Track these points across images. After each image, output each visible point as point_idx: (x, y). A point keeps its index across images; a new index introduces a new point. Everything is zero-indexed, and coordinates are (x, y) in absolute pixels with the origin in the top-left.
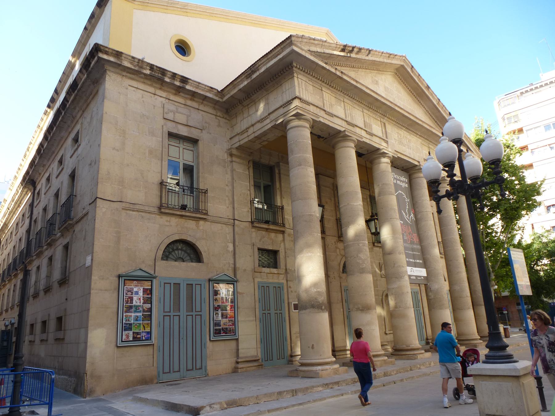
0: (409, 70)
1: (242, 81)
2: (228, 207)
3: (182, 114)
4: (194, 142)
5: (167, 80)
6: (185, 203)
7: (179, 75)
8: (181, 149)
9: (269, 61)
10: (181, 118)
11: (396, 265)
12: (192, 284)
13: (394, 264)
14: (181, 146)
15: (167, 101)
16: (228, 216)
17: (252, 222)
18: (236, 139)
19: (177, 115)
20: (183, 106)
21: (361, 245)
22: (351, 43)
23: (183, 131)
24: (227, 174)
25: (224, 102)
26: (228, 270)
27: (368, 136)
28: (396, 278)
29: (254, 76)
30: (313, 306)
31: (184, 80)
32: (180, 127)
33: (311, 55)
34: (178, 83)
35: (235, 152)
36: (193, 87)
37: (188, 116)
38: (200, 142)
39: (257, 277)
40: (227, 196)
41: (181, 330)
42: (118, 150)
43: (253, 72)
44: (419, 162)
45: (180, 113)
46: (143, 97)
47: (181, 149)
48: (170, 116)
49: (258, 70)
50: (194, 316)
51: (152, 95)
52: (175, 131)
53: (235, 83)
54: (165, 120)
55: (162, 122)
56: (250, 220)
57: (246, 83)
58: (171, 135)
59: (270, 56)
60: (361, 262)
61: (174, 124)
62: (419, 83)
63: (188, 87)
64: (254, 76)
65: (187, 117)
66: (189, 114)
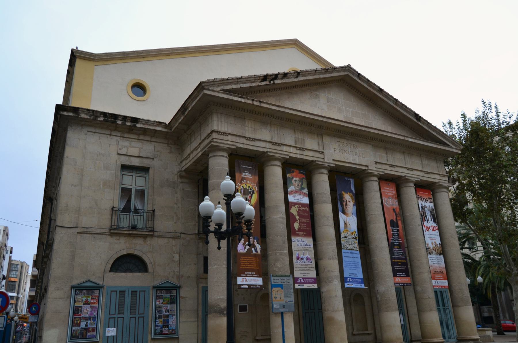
0: (356, 78)
1: (180, 116)
2: (175, 223)
3: (135, 147)
4: (145, 170)
5: (119, 122)
6: (136, 224)
7: (129, 117)
8: (134, 177)
9: (193, 102)
10: (134, 151)
11: (325, 271)
12: (137, 291)
13: (324, 269)
14: (134, 174)
15: (122, 138)
16: (175, 231)
17: (199, 234)
18: (184, 163)
19: (130, 149)
20: (136, 140)
21: (278, 254)
22: (270, 72)
23: (136, 162)
24: (176, 193)
25: (173, 132)
26: (173, 277)
27: (298, 152)
28: (326, 282)
29: (186, 113)
30: (216, 312)
31: (135, 120)
32: (132, 158)
33: (224, 94)
34: (128, 124)
35: (184, 173)
36: (143, 124)
37: (140, 149)
38: (150, 169)
39: (202, 283)
40: (175, 213)
41: (125, 330)
42: (76, 186)
43: (186, 110)
44: (367, 166)
45: (133, 147)
46: (100, 139)
47: (134, 177)
48: (124, 151)
49: (188, 108)
50: (116, 319)
51: (109, 136)
52: (127, 163)
53: (176, 117)
54: (119, 156)
55: (117, 157)
56: (197, 232)
57: (182, 118)
58: (124, 167)
59: (192, 97)
60: (276, 269)
61: (127, 158)
62: (369, 88)
63: (138, 125)
64: (186, 113)
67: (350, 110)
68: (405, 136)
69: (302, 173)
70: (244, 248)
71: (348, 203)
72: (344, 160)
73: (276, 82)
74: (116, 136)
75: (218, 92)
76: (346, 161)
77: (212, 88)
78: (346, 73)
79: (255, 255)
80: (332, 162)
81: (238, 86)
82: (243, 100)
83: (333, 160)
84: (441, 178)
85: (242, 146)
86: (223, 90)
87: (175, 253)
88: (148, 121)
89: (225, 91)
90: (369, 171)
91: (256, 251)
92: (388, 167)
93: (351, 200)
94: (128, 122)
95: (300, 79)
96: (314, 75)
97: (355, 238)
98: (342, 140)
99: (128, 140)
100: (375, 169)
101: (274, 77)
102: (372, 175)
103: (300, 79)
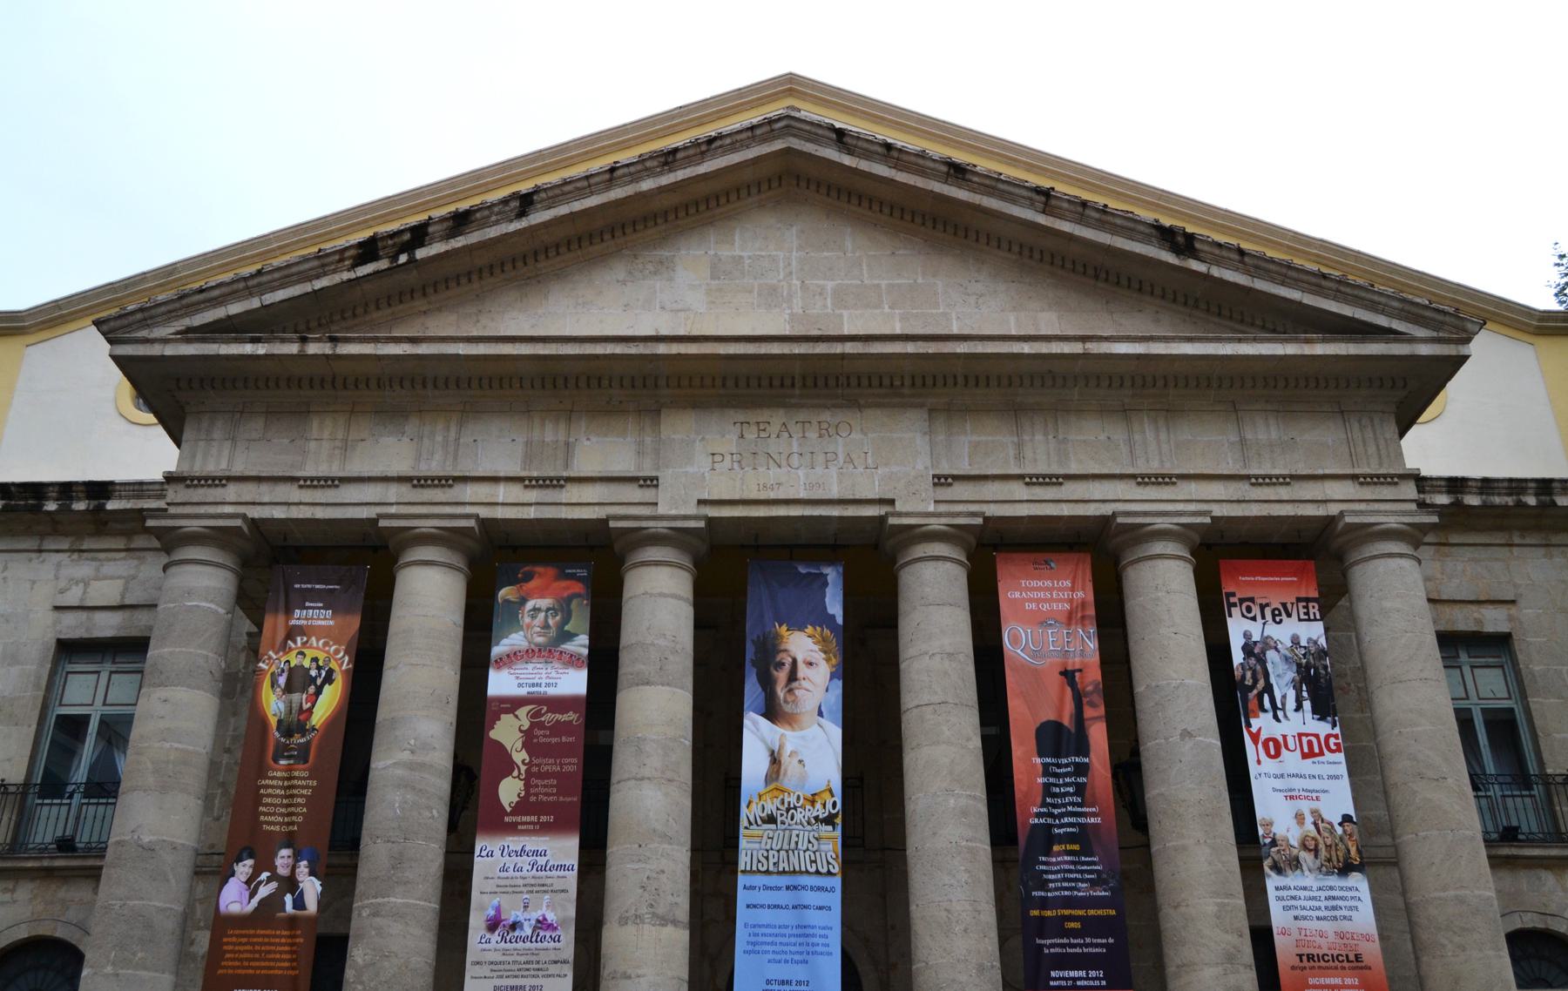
0: (831, 154)
2: (218, 819)
3: (112, 578)
5: (51, 506)
7: (76, 483)
8: (104, 676)
10: (106, 591)
15: (75, 556)
19: (95, 585)
20: (123, 554)
23: (107, 626)
24: (235, 714)
27: (533, 495)
31: (99, 490)
32: (100, 617)
33: (189, 341)
34: (80, 506)
36: (128, 498)
40: (223, 784)
44: (891, 502)
45: (105, 578)
46: (5, 568)
48: (72, 598)
51: (34, 555)
54: (57, 614)
55: (52, 615)
61: (83, 615)
62: (902, 177)
63: (111, 505)
65: (127, 582)
66: (132, 572)
67: (830, 285)
68: (1084, 339)
69: (572, 577)
70: (247, 894)
71: (802, 670)
72: (763, 496)
73: (421, 254)
74: (58, 551)
75: (165, 341)
76: (772, 495)
77: (144, 333)
78: (778, 145)
79: (292, 922)
80: (692, 510)
81: (255, 303)
82: (261, 349)
83: (701, 502)
84: (1367, 493)
85: (279, 513)
86: (189, 330)
87: (199, 929)
88: (141, 483)
89: (188, 335)
90: (892, 521)
91: (299, 903)
92: (1018, 490)
93: (819, 657)
94: (79, 499)
95: (538, 217)
96: (608, 189)
97: (829, 820)
98: (763, 415)
99: (93, 559)
100: (931, 508)
101: (407, 237)
102: (913, 535)
103: (538, 217)
